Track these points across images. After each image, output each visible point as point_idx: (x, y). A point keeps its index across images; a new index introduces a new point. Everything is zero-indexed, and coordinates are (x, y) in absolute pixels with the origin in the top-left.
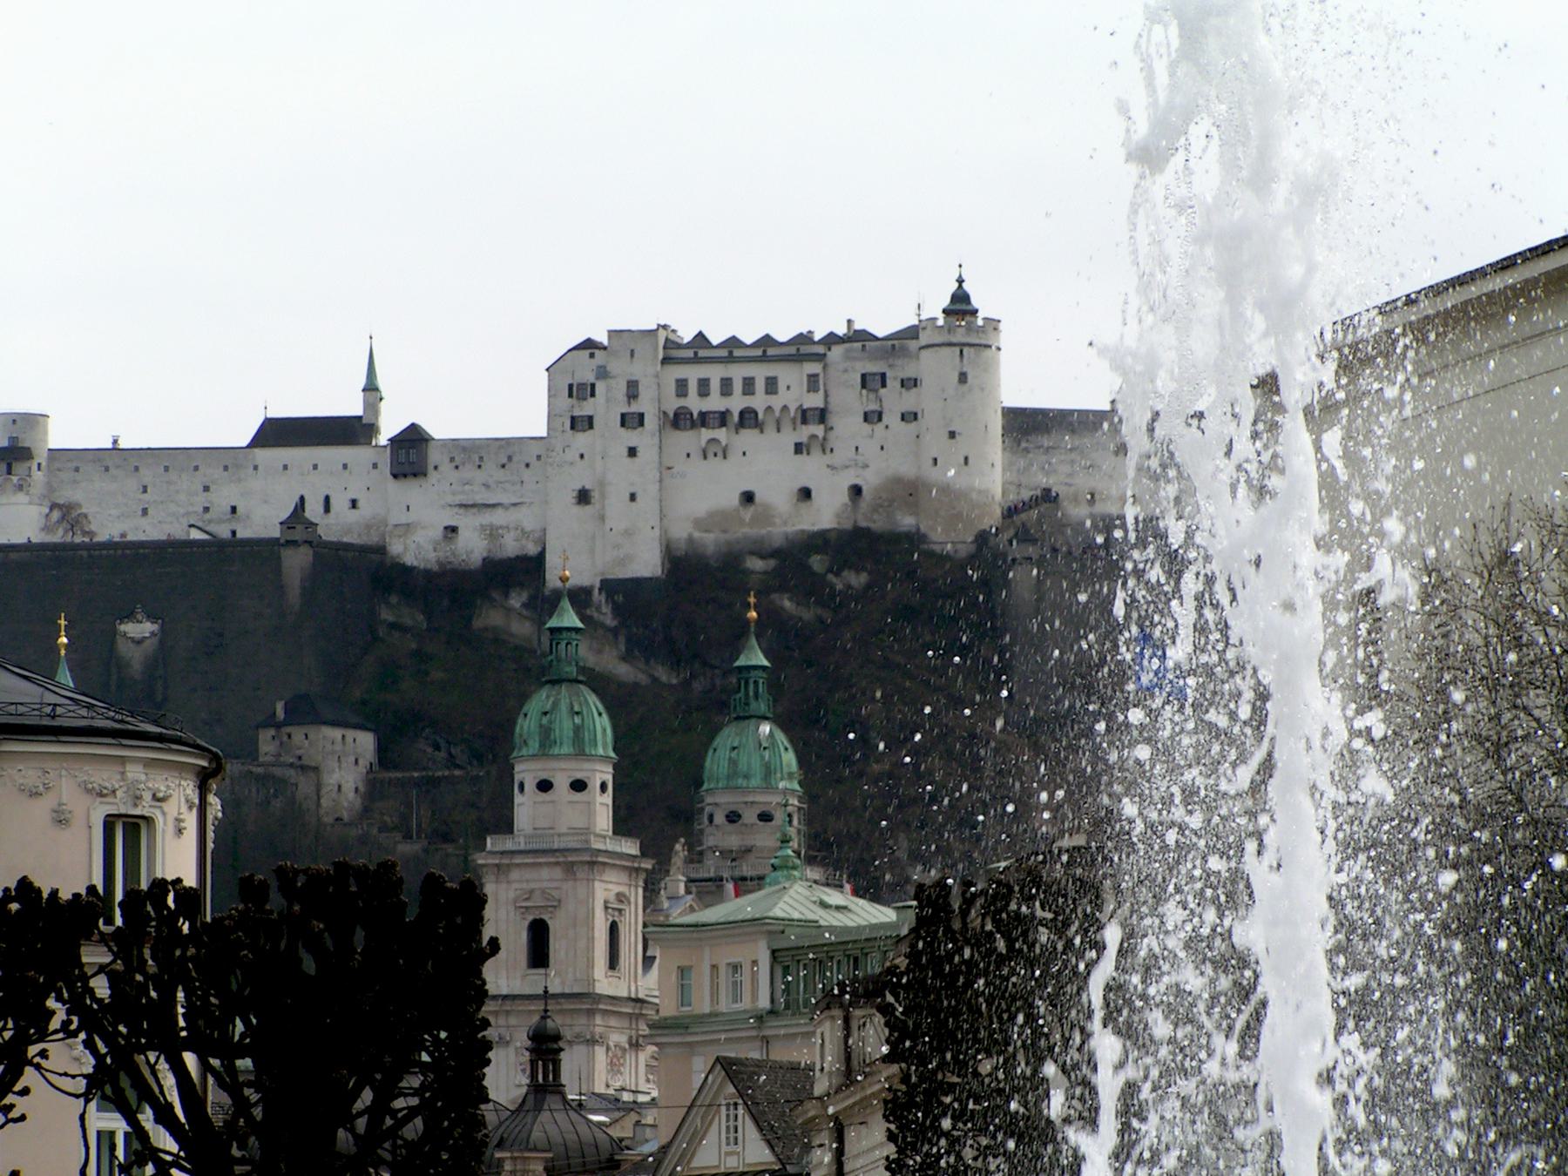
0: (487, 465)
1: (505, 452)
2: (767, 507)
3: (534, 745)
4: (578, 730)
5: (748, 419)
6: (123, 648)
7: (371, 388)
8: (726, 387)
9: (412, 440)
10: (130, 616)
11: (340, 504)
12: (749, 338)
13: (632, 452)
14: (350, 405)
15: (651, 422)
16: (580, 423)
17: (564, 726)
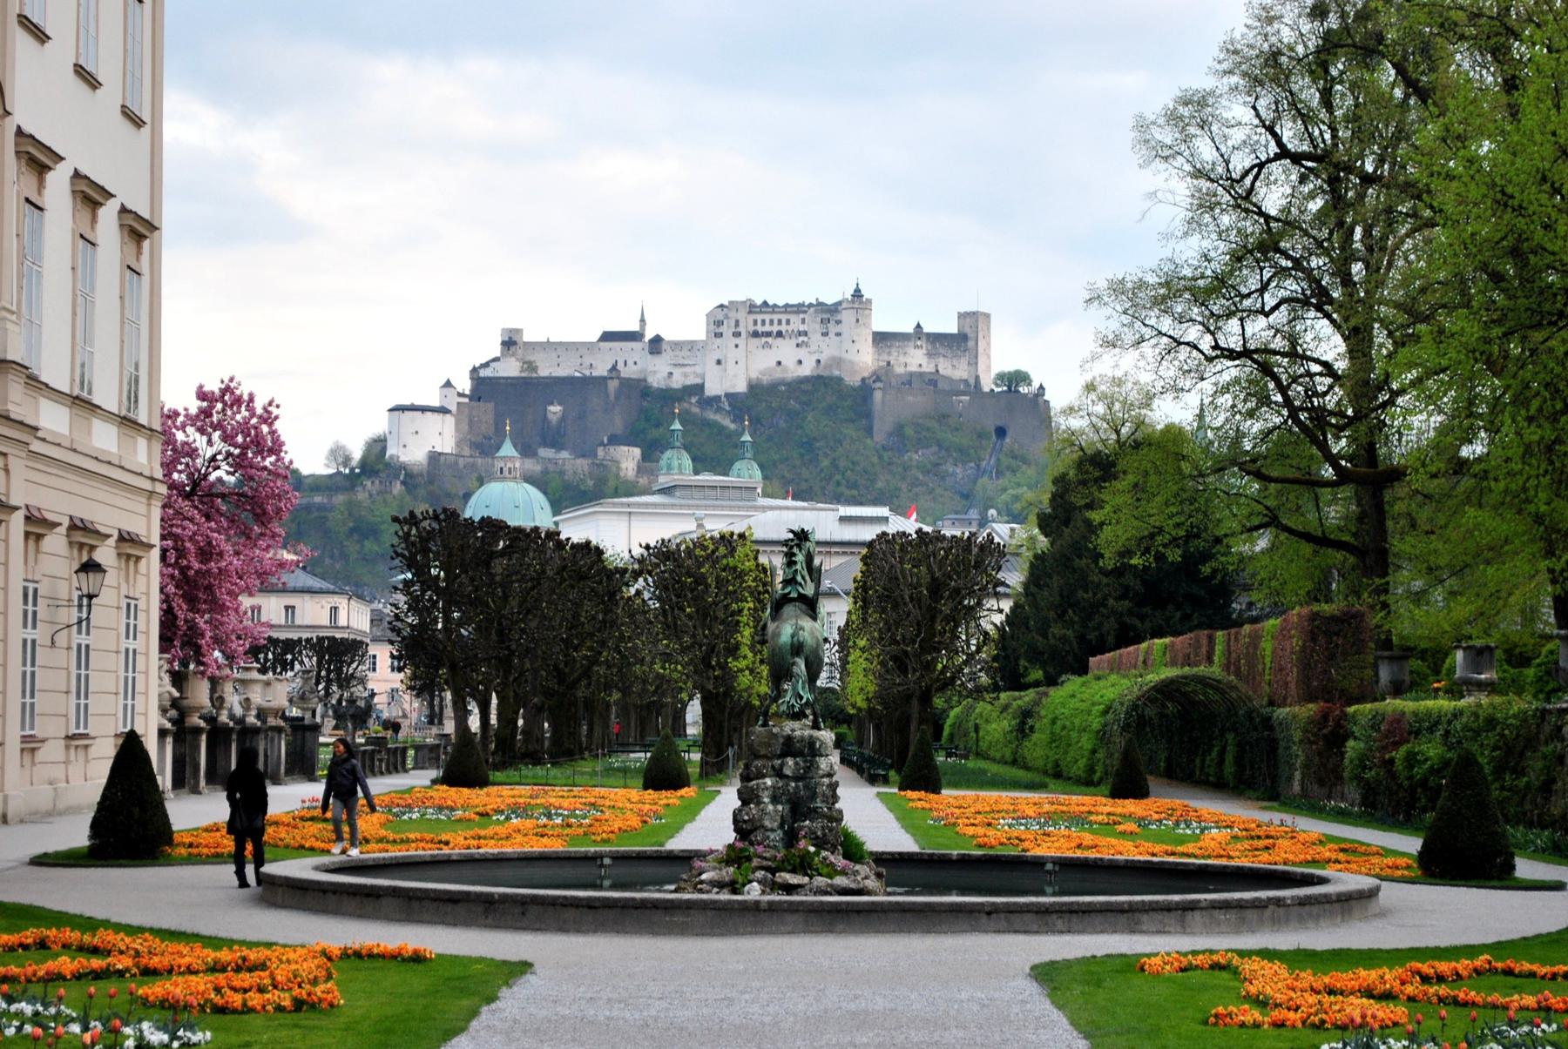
0: (685, 349)
1: (691, 345)
3: (664, 471)
4: (680, 465)
5: (780, 334)
6: (550, 416)
7: (643, 321)
8: (772, 322)
9: (657, 340)
10: (552, 404)
11: (630, 363)
12: (781, 303)
13: (737, 346)
14: (635, 327)
15: (744, 335)
16: (719, 335)
17: (675, 463)
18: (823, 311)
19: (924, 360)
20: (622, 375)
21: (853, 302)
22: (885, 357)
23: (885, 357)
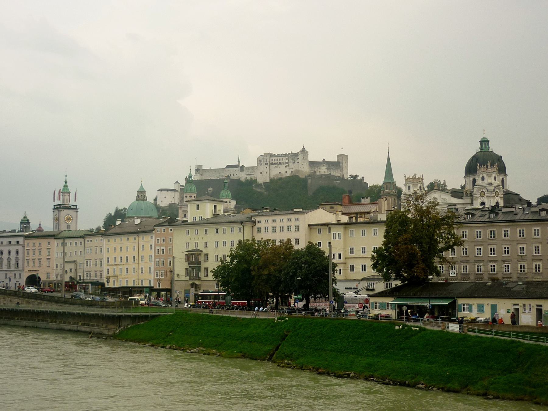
1: (253, 168)
2: (282, 174)
4: (191, 189)
5: (280, 163)
7: (239, 161)
8: (277, 159)
9: (243, 166)
10: (209, 188)
11: (235, 174)
13: (266, 168)
15: (268, 164)
16: (261, 164)
17: (189, 189)
18: (293, 156)
19: (326, 171)
20: (232, 177)
21: (302, 152)
22: (313, 170)
23: (313, 170)
